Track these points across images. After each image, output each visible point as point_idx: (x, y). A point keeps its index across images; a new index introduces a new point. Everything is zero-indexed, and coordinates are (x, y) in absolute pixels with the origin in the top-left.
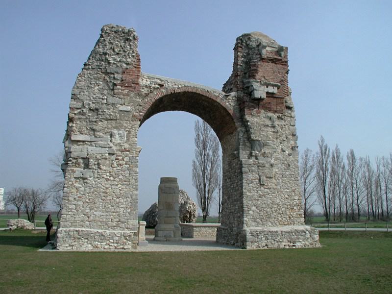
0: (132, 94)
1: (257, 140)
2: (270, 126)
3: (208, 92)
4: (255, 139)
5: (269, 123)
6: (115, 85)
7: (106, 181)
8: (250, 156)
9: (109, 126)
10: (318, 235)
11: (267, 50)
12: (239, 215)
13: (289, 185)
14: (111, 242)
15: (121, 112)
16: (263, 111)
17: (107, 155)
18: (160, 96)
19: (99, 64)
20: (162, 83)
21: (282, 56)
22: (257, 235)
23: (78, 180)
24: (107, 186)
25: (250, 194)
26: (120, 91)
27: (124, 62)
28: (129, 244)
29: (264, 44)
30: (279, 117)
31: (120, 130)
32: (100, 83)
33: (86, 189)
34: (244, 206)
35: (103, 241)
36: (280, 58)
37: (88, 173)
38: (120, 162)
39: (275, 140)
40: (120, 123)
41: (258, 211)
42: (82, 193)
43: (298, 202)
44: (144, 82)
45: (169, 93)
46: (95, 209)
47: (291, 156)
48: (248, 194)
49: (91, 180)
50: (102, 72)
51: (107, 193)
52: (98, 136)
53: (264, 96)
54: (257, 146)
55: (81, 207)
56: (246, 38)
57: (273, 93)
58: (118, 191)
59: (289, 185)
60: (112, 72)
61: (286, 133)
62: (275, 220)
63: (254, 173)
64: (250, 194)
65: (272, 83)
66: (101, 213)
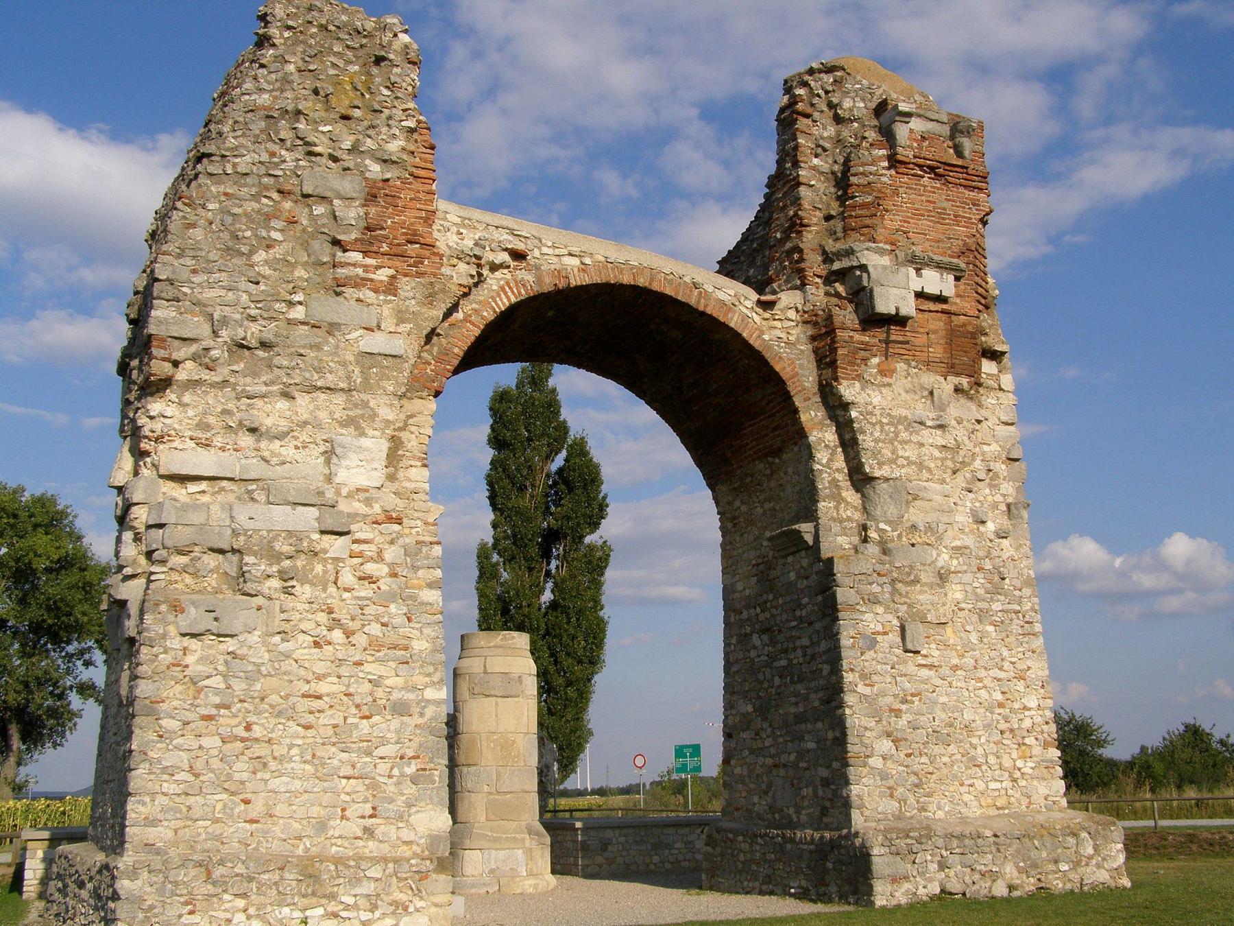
0: (407, 286)
1: (887, 480)
2: (929, 423)
3: (696, 286)
4: (877, 474)
5: (923, 410)
6: (336, 242)
7: (317, 644)
9: (323, 415)
10: (1120, 846)
11: (911, 131)
12: (824, 772)
13: (1005, 653)
14: (347, 907)
15: (367, 361)
16: (901, 366)
17: (316, 536)
18: (513, 300)
19: (265, 157)
20: (520, 246)
21: (967, 153)
22: (911, 852)
23: (194, 644)
24: (320, 668)
25: (867, 691)
26: (360, 271)
27: (372, 154)
28: (417, 910)
29: (903, 107)
30: (958, 390)
31: (363, 434)
32: (276, 235)
33: (232, 682)
34: (850, 739)
35: (314, 900)
36: (960, 162)
37: (240, 613)
38: (370, 568)
39: (947, 476)
40: (365, 404)
41: (902, 755)
42: (217, 700)
43: (1038, 720)
44: (452, 239)
45: (547, 287)
46: (273, 765)
47: (1005, 542)
48: (861, 688)
50: (280, 192)
51: (319, 697)
52: (275, 460)
53: (908, 307)
55: (215, 763)
56: (829, 79)
57: (940, 299)
58: (367, 687)
59: (1005, 653)
60: (328, 194)
61: (983, 454)
62: (964, 789)
63: (880, 610)
64: (867, 691)
65: (936, 258)
66: (297, 785)
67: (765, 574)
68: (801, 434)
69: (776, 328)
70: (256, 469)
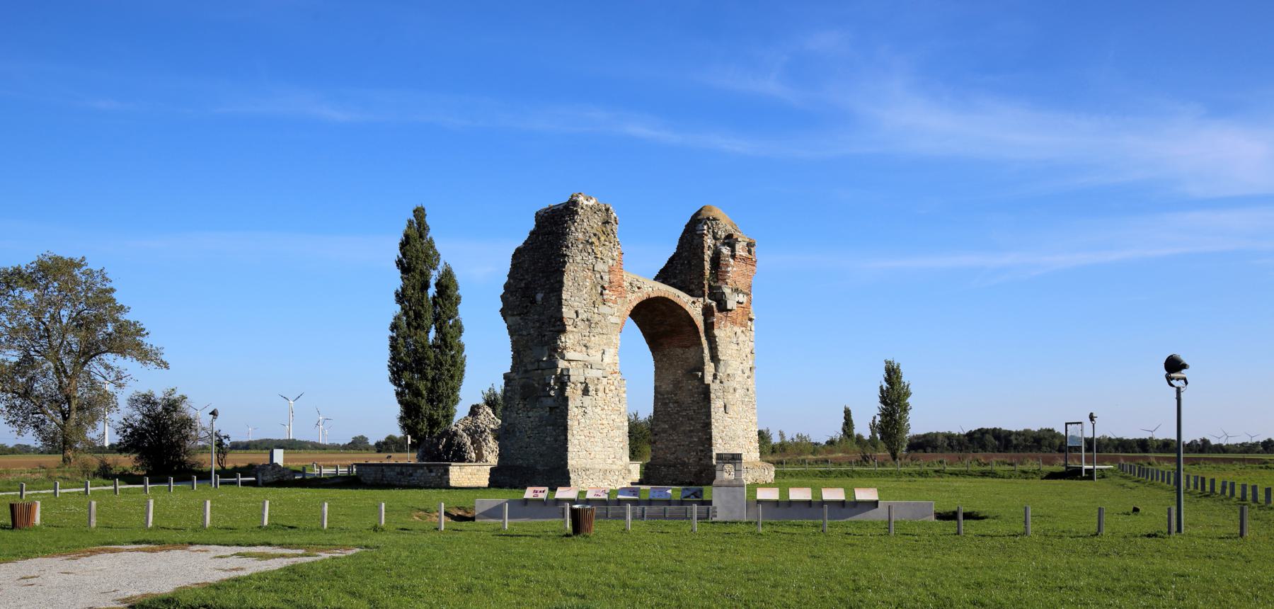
8: (715, 376)
37: (587, 400)
49: (589, 410)
54: (722, 367)
67: (677, 384)
68: (700, 344)
69: (694, 308)
70: (586, 358)
